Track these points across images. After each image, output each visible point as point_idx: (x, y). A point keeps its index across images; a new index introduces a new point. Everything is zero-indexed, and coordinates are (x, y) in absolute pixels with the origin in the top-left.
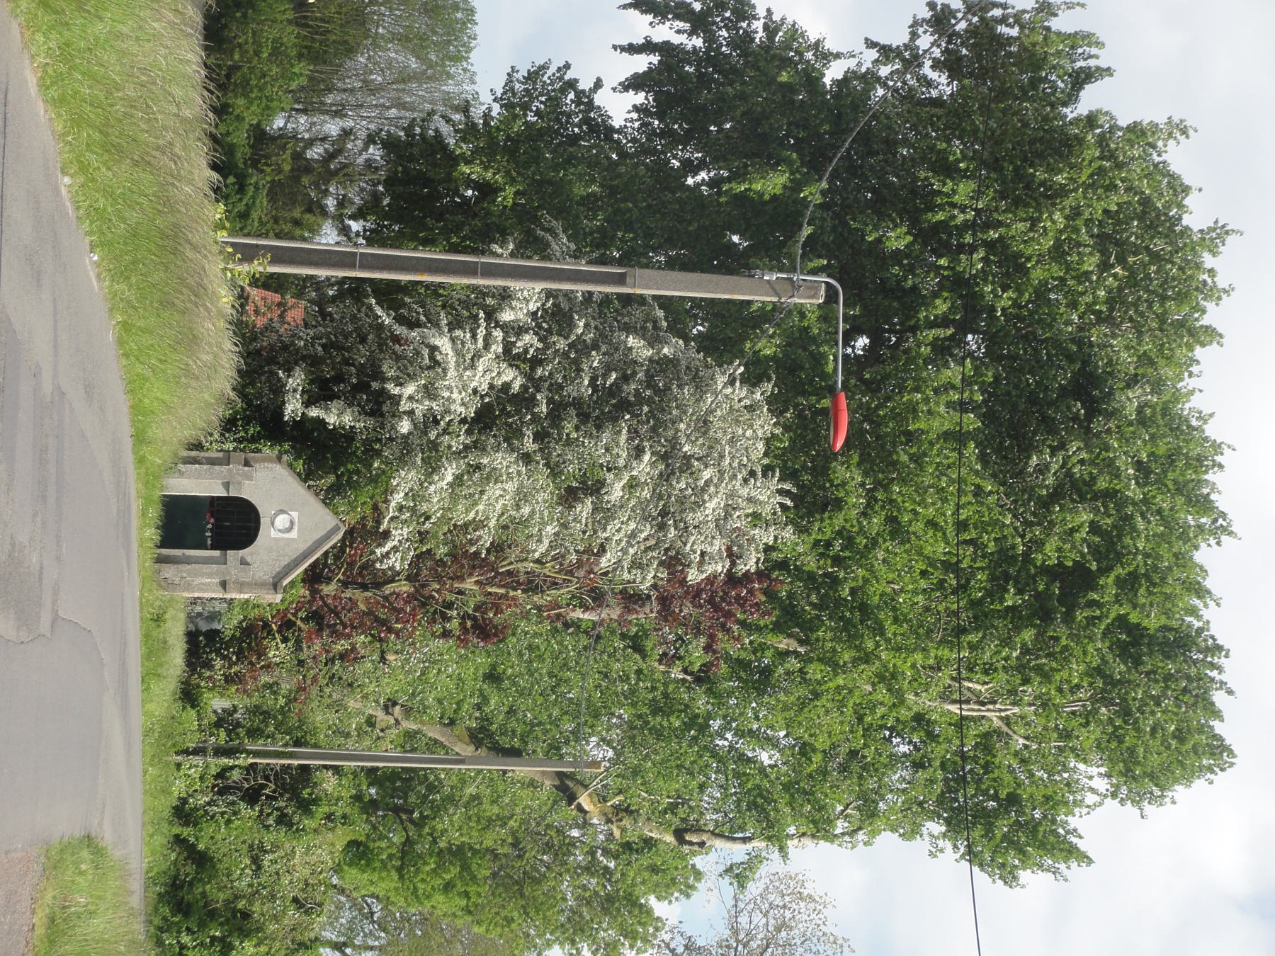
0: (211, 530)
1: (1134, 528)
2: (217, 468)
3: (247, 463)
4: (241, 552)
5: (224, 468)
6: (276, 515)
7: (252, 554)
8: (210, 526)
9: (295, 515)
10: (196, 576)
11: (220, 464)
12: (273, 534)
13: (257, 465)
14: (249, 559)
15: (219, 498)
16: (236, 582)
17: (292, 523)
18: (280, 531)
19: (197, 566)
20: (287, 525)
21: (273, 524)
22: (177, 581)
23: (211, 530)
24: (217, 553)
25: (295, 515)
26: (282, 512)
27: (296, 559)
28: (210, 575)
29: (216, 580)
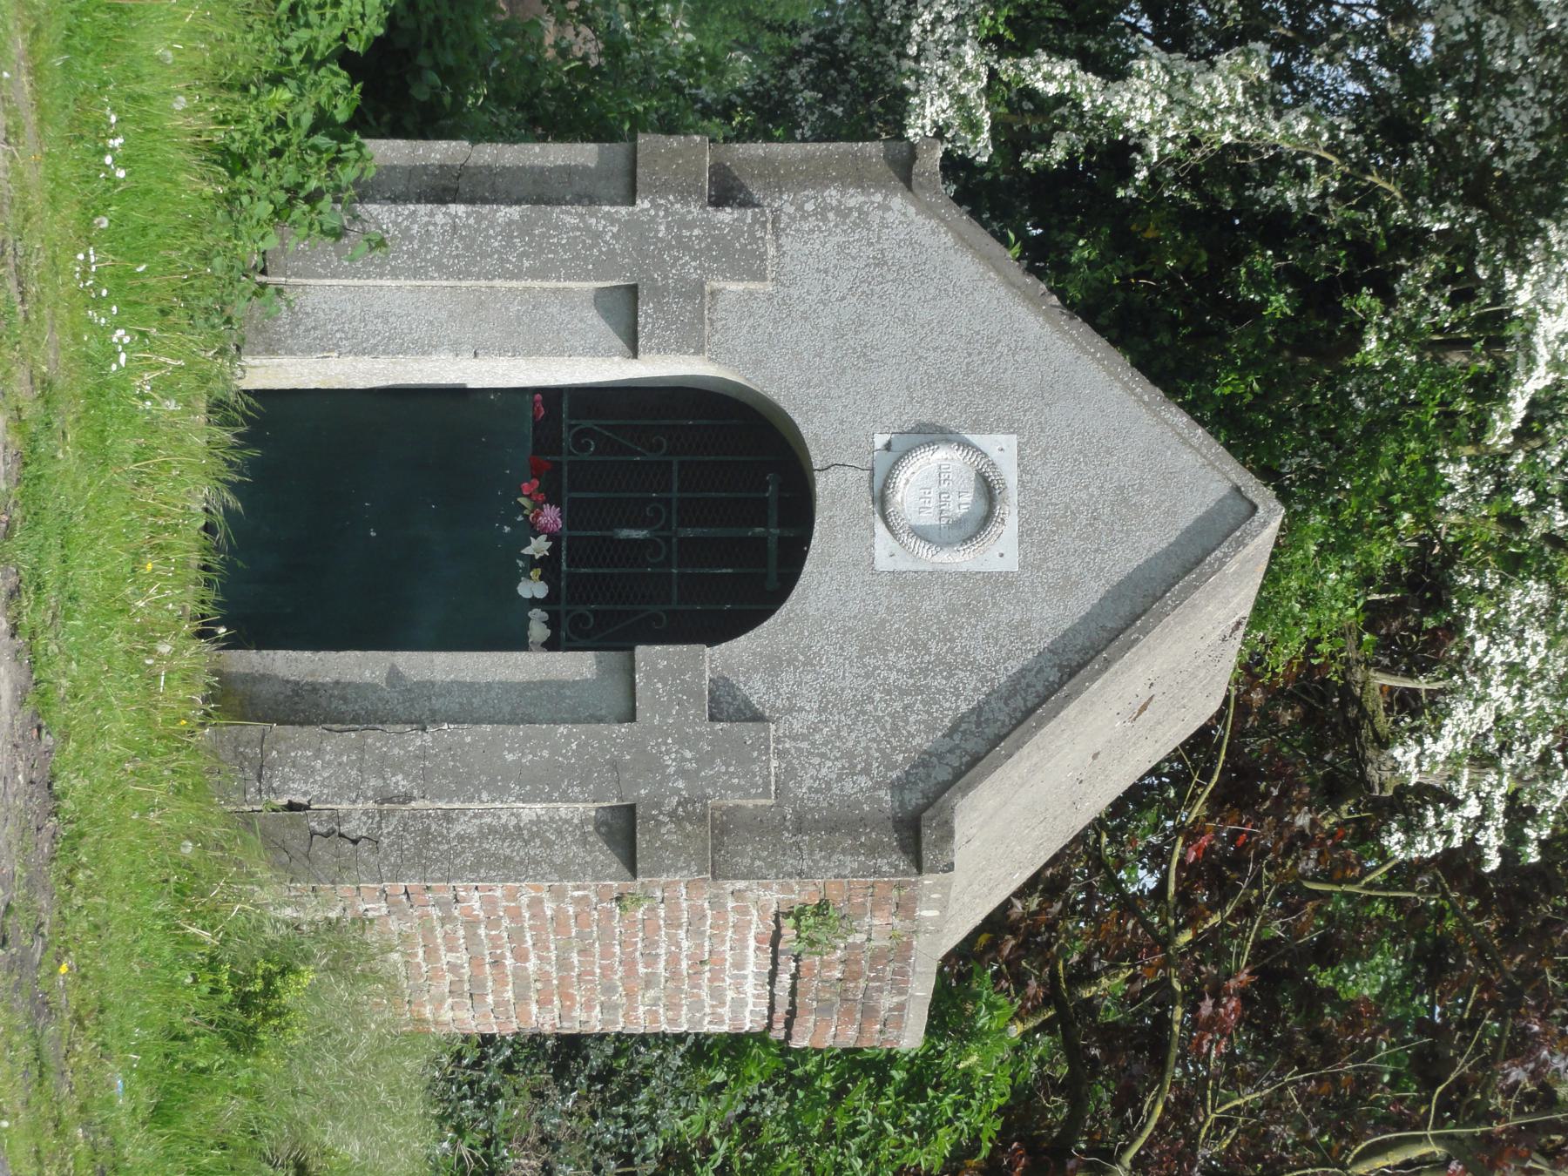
0: (547, 567)
1: (1434, 273)
2: (568, 216)
3: (726, 191)
4: (715, 658)
5: (608, 219)
6: (897, 454)
7: (773, 665)
8: (538, 547)
9: (1001, 448)
10: (464, 785)
11: (588, 199)
12: (885, 552)
13: (786, 203)
14: (756, 691)
15: (382, 136)
16: (690, 813)
17: (988, 490)
18: (920, 533)
19: (468, 734)
20: (964, 501)
21: (881, 500)
22: (357, 813)
23: (547, 567)
24: (579, 666)
25: (1001, 448)
26: (931, 434)
27: (1018, 683)
28: (540, 783)
29: (579, 809)
